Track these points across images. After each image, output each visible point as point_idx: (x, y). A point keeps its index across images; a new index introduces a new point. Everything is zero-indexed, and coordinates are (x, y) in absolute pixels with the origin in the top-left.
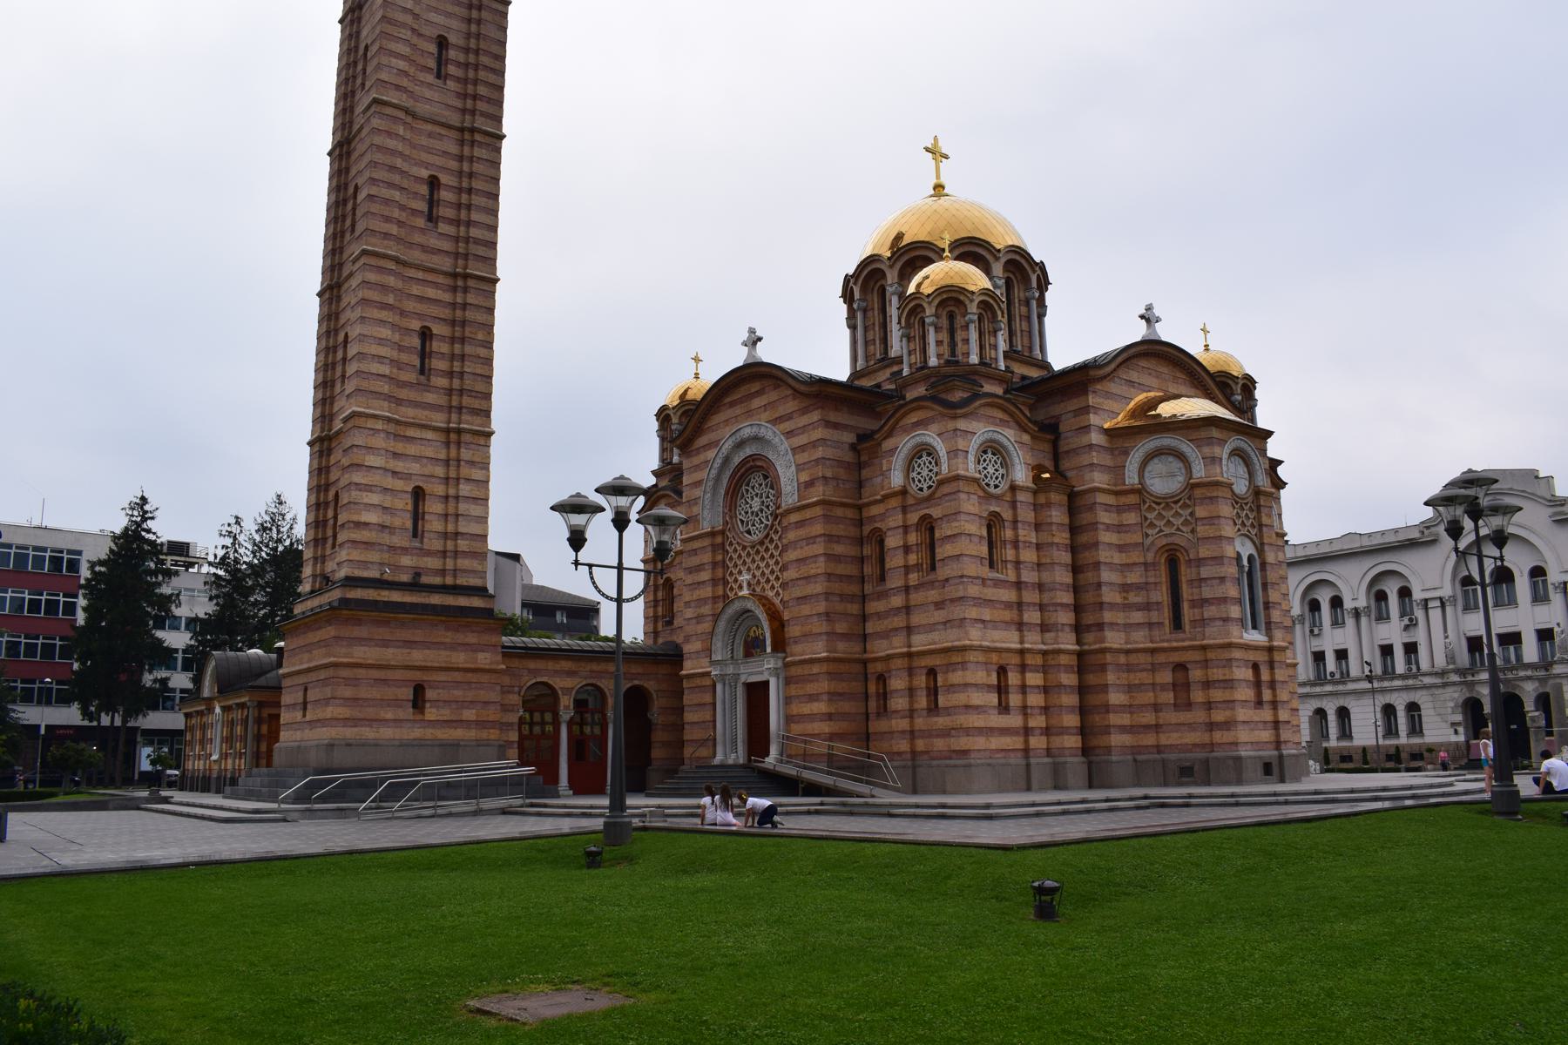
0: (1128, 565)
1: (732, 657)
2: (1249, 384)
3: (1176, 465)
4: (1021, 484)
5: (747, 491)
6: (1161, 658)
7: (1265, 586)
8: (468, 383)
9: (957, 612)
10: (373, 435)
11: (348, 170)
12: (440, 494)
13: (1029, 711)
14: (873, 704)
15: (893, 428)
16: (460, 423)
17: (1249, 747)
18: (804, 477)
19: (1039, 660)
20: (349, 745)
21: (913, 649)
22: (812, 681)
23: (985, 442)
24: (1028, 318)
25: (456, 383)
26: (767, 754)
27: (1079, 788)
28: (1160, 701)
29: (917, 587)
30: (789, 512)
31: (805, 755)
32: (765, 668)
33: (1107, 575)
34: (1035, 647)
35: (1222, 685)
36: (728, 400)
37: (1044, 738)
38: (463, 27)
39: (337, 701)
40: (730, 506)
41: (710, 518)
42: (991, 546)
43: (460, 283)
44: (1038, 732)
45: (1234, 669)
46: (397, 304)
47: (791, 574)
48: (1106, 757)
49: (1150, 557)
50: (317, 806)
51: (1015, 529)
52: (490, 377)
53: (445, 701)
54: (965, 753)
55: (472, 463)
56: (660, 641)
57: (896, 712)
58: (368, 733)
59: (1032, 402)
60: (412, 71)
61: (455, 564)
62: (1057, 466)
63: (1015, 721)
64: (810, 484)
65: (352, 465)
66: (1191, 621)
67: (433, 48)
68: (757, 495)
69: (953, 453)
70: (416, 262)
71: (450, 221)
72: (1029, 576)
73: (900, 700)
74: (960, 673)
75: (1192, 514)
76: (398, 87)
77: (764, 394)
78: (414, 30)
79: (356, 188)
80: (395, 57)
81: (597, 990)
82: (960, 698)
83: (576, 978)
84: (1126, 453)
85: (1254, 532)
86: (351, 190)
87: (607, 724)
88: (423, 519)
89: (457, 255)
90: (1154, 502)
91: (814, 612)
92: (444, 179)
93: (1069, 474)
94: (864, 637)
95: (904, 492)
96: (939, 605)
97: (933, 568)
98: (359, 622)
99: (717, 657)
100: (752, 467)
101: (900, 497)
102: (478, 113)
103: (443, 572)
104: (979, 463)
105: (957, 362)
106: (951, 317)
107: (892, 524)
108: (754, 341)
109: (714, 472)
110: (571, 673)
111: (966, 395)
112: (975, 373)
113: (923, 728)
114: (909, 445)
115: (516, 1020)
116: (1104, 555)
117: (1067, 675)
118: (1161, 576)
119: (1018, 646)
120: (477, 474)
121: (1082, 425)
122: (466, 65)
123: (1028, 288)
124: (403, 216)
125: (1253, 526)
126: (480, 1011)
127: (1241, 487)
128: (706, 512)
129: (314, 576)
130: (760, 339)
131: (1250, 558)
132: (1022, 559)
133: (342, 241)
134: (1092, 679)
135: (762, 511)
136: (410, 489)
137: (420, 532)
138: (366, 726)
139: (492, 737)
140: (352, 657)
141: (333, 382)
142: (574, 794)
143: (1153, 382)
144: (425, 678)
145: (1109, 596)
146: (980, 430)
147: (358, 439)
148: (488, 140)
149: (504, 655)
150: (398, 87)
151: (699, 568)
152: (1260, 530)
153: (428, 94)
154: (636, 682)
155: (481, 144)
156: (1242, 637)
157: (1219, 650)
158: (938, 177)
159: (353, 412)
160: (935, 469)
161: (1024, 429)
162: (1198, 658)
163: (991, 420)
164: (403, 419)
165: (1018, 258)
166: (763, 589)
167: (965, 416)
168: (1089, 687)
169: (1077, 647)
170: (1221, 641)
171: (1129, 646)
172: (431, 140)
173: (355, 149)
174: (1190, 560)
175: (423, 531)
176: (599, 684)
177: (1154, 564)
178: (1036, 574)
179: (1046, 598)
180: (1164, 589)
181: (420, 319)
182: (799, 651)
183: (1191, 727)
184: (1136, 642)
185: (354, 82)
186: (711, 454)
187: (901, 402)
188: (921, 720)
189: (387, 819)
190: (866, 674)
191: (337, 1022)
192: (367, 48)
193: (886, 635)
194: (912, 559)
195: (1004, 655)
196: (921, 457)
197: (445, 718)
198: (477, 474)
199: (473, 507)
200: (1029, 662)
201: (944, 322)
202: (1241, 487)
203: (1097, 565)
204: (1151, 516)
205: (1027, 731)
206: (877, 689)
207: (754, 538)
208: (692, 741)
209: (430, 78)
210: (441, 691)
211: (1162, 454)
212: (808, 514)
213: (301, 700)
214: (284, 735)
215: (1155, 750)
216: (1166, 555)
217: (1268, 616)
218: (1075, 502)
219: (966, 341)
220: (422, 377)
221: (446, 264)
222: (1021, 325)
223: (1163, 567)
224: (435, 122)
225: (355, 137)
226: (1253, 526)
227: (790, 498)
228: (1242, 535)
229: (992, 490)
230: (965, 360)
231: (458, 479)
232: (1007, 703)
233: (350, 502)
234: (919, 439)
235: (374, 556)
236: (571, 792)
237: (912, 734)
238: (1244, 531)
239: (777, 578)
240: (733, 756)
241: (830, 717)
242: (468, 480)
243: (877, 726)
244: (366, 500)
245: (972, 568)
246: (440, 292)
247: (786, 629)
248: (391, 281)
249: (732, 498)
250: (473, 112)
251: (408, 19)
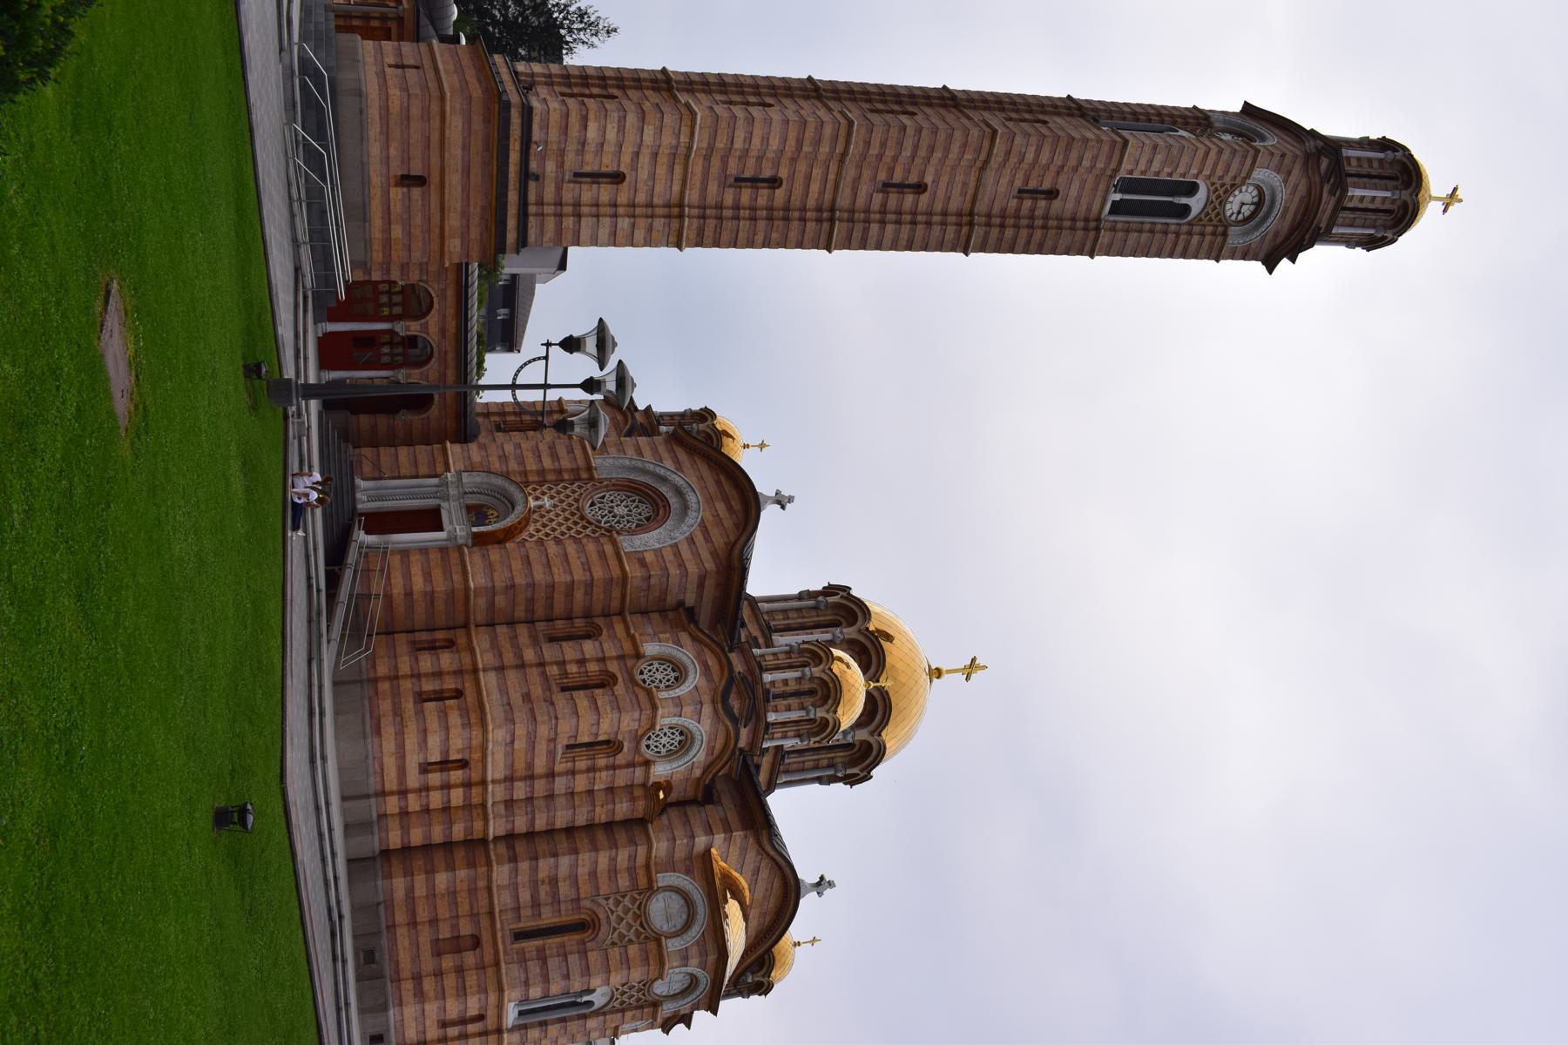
0: (577, 883)
1: (466, 493)
2: (763, 988)
3: (679, 922)
4: (652, 771)
5: (634, 501)
6: (485, 922)
7: (563, 1020)
8: (729, 225)
9: (521, 715)
10: (674, 133)
11: (930, 105)
12: (619, 198)
13: (424, 794)
14: (424, 636)
16: (688, 217)
17: (398, 1018)
18: (649, 557)
19: (476, 800)
20: (361, 112)
21: (481, 675)
22: (444, 574)
23: (691, 732)
24: (816, 768)
25: (728, 213)
26: (368, 533)
27: (347, 850)
28: (441, 924)
29: (545, 677)
30: (614, 543)
31: (369, 571)
32: (456, 526)
33: (565, 861)
34: (490, 796)
35: (460, 985)
36: (723, 478)
37: (397, 810)
38: (1068, 214)
39: (406, 99)
40: (618, 485)
41: (606, 465)
42: (589, 745)
43: (825, 215)
44: (403, 804)
45: (477, 996)
46: (802, 155)
47: (552, 548)
48: (380, 875)
49: (586, 903)
50: (297, 81)
51: (607, 768)
52: (735, 246)
53: (409, 207)
54: (378, 732)
55: (650, 229)
56: (480, 420)
57: (417, 660)
58: (374, 131)
59: (733, 775)
60: (1025, 166)
61: (548, 215)
62: (671, 805)
63: (413, 780)
64: (642, 563)
65: (643, 112)
66: (523, 949)
67: (1046, 186)
68: (630, 511)
69: (679, 702)
70: (844, 172)
71: (884, 204)
72: (560, 784)
73: (429, 664)
74: (459, 722)
75: (630, 941)
76: (1008, 153)
77: (730, 514)
78: (1062, 167)
79: (913, 114)
80: (1036, 150)
81: (131, 399)
82: (433, 723)
83: (141, 377)
84: (688, 872)
85: (616, 1004)
86: (910, 109)
87: (392, 369)
88: (593, 183)
89: (852, 211)
90: (641, 903)
92: (924, 198)
93: (664, 818)
94: (491, 625)
95: (638, 656)
96: (527, 697)
97: (564, 689)
98: (487, 120)
99: (466, 478)
100: (657, 505)
101: (633, 652)
102: (988, 229)
103: (540, 203)
104: (670, 728)
105: (768, 701)
106: (811, 692)
107: (606, 646)
108: (781, 501)
109: (651, 467)
110: (443, 331)
111: (736, 711)
112: (758, 719)
113: (401, 689)
114: (685, 659)
115: (102, 330)
116: (585, 858)
117: (462, 829)
118: (567, 915)
119: (489, 778)
120: (639, 234)
121: (713, 827)
122: (1032, 217)
123: (847, 765)
124: (887, 159)
125: (623, 1003)
126: (108, 294)
127: (660, 988)
128: (610, 461)
129: (532, 75)
130: (783, 507)
131: (590, 1003)
132: (577, 776)
133: (862, 100)
134: (460, 854)
135: (614, 516)
137: (579, 179)
138: (382, 127)
139: (375, 255)
140: (451, 115)
141: (726, 93)
142: (319, 338)
143: (759, 894)
144: (432, 187)
145: (545, 865)
146: (703, 727)
147: (669, 119)
148: (963, 239)
149: (459, 266)
150: (1008, 153)
151: (555, 456)
152: (618, 1011)
153: (1004, 181)
156: (510, 1001)
157: (495, 980)
158: (949, 672)
159: (696, 114)
160: (662, 686)
161: (706, 770)
162: (486, 960)
163: (713, 738)
164: (691, 162)
165: (874, 753)
166: (536, 521)
167: (716, 711)
168: (451, 852)
169: (491, 837)
170: (505, 981)
171: (495, 889)
172: (960, 186)
173: (950, 112)
174: (584, 943)
175: (580, 183)
176: (433, 360)
177: (579, 908)
178: (563, 792)
179: (540, 803)
180: (557, 920)
181: (789, 176)
182: (474, 560)
183: (416, 958)
184: (499, 895)
185: (1013, 110)
186: (669, 464)
187: (727, 649)
188: (410, 686)
189: (286, 152)
190: (454, 628)
191: (93, 161)
192: (1045, 122)
193: (495, 646)
194: (573, 668)
195: (480, 765)
196: (674, 670)
197: (392, 204)
198: (639, 234)
199: (607, 231)
200: (473, 791)
201: (806, 686)
202: (660, 988)
203: (575, 851)
204: (627, 901)
205: (403, 793)
206: (439, 640)
207: (587, 510)
208: (378, 455)
209: (1018, 183)
210: (420, 203)
211: (688, 908)
212: (613, 562)
213: (406, 62)
214: (369, 44)
215: (390, 924)
216: (589, 919)
217: (532, 1026)
218: (637, 826)
219: (789, 709)
220: (733, 180)
221: (843, 201)
222: (809, 761)
223: (577, 917)
224: (977, 188)
225: (961, 111)
226: (623, 1003)
227: (628, 544)
228: (613, 992)
229: (644, 742)
230: (770, 708)
231: (634, 216)
232: (431, 771)
233: (606, 111)
234: (691, 667)
235: (554, 135)
236: (321, 335)
237: (394, 678)
238: (617, 995)
239: (547, 535)
240: (364, 498)
241: (409, 594)
242: (633, 226)
243: (402, 640)
244: (609, 127)
245: (565, 728)
246: (816, 196)
247: (496, 546)
248: (825, 149)
249: (623, 486)
250: (988, 224)
251: (1072, 162)
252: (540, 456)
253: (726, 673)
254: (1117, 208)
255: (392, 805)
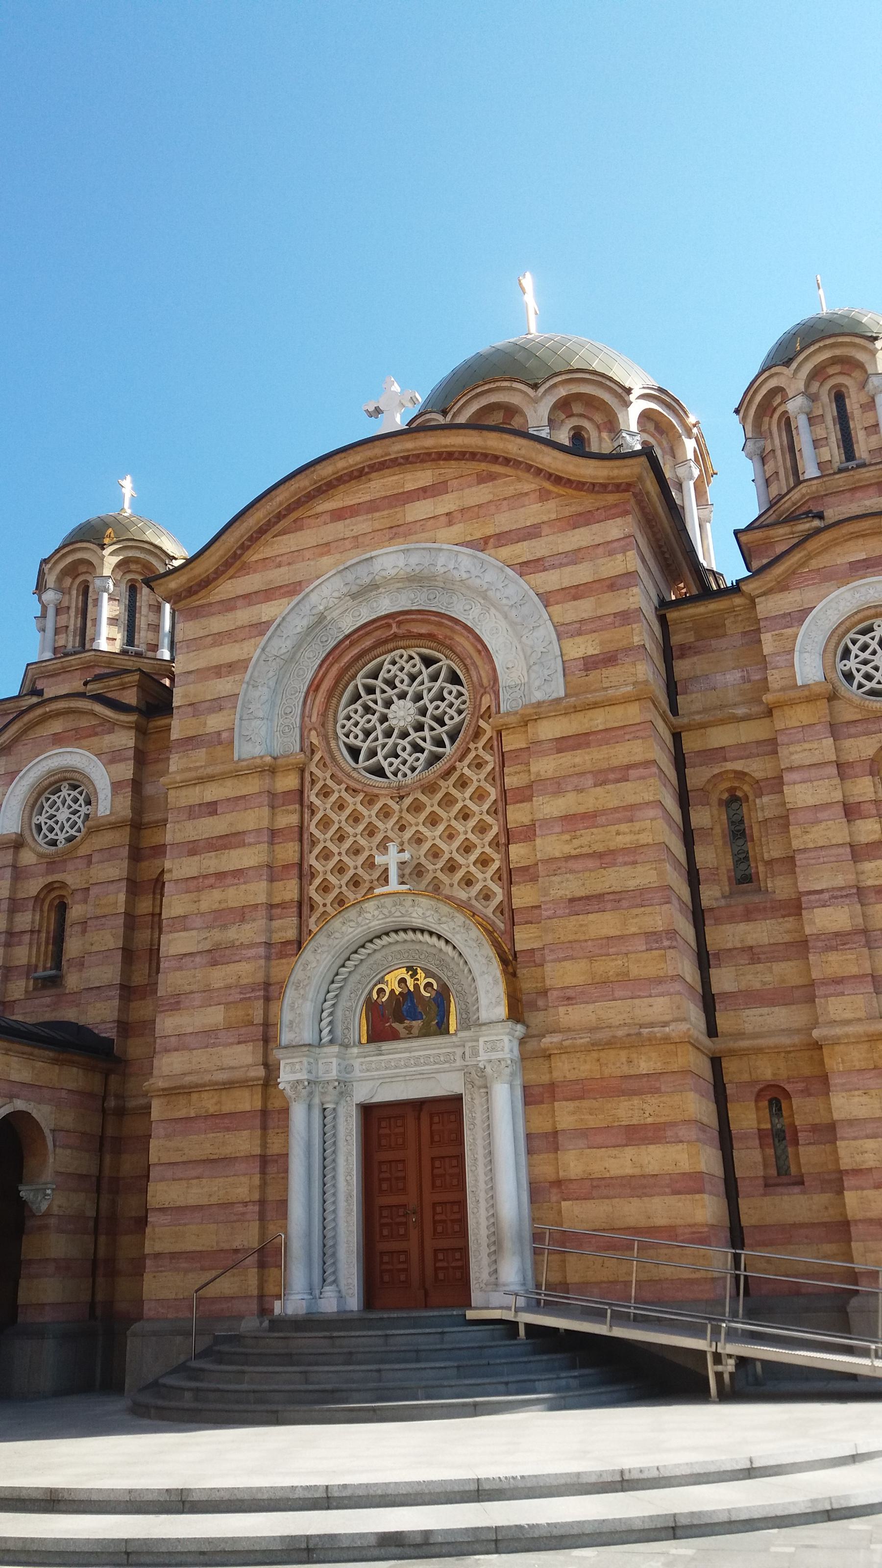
15: (793, 572)
91: (633, 930)
95: (833, 697)
100: (395, 637)
154: (20, 1105)
252: (221, 876)
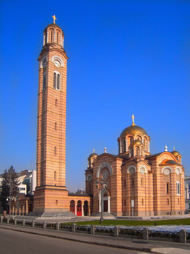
36: (101, 158)
60: (52, 105)
78: (52, 98)
127: (178, 174)
131: (179, 184)
136: (54, 171)
153: (55, 109)
155: (63, 117)
163: (142, 164)
202: (178, 174)
209: (55, 106)
217: (181, 192)
221: (58, 137)
224: (55, 114)
229: (142, 174)
253: (133, 161)
254: (58, 88)
255: (147, 209)
